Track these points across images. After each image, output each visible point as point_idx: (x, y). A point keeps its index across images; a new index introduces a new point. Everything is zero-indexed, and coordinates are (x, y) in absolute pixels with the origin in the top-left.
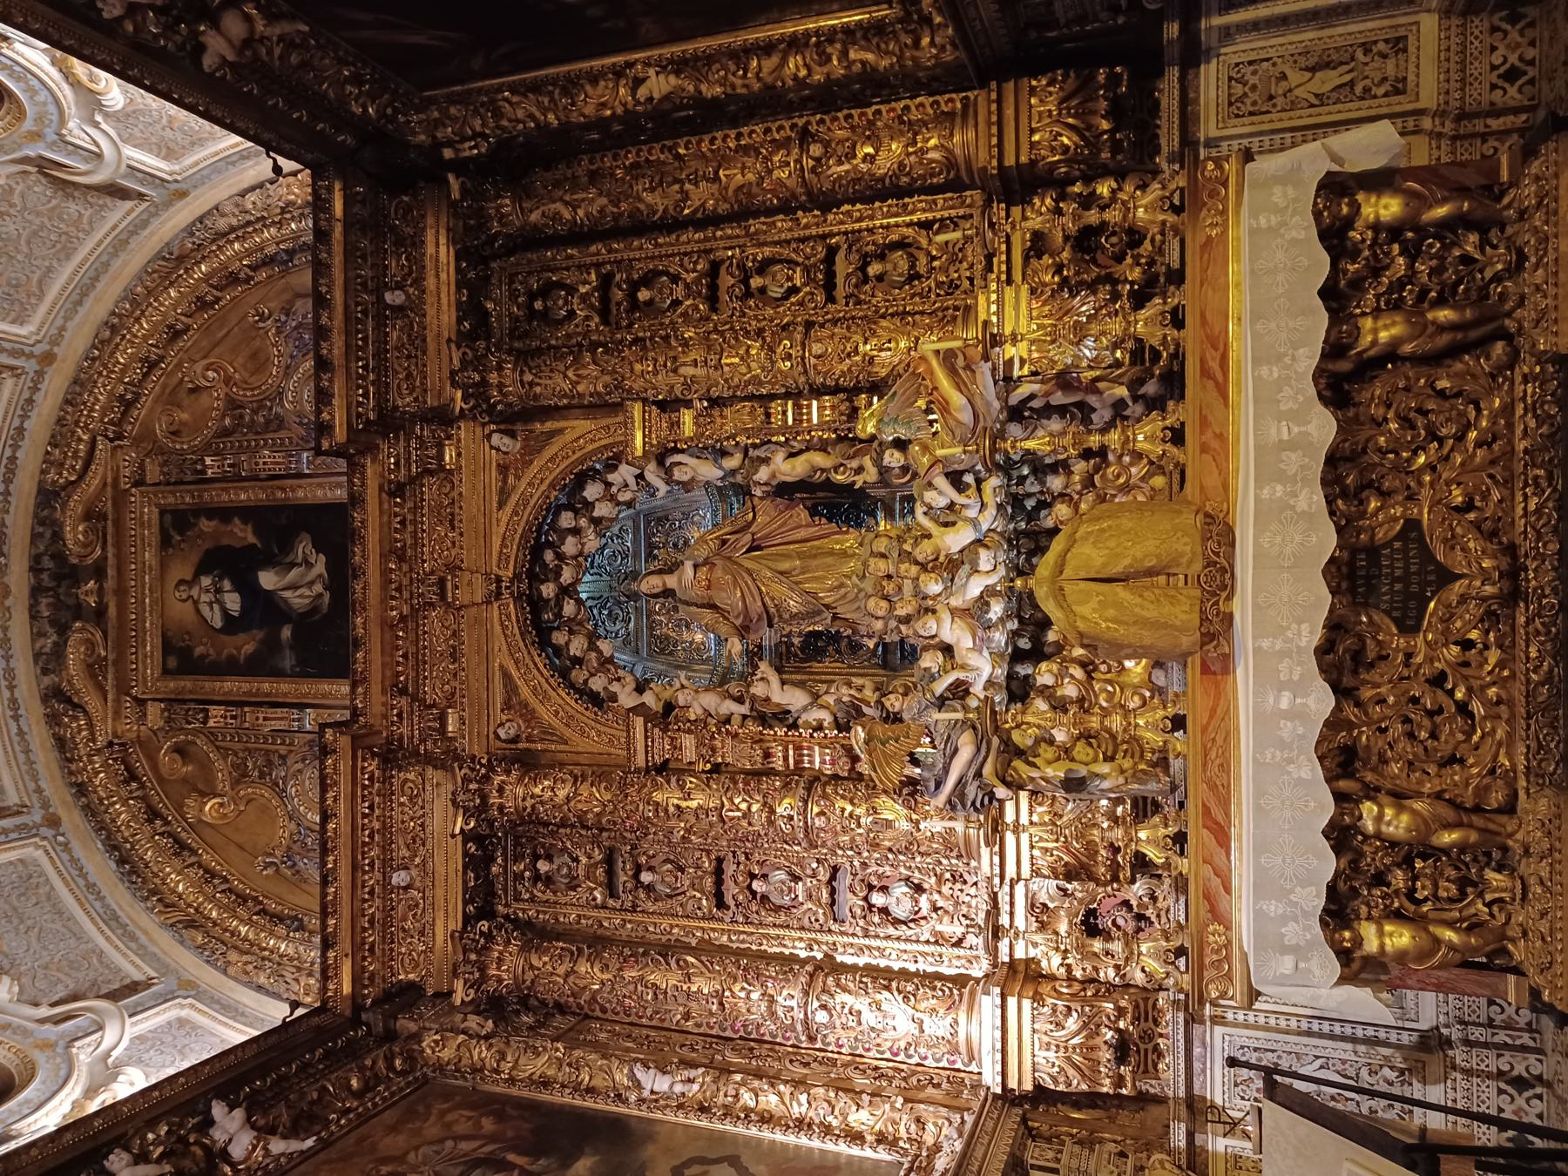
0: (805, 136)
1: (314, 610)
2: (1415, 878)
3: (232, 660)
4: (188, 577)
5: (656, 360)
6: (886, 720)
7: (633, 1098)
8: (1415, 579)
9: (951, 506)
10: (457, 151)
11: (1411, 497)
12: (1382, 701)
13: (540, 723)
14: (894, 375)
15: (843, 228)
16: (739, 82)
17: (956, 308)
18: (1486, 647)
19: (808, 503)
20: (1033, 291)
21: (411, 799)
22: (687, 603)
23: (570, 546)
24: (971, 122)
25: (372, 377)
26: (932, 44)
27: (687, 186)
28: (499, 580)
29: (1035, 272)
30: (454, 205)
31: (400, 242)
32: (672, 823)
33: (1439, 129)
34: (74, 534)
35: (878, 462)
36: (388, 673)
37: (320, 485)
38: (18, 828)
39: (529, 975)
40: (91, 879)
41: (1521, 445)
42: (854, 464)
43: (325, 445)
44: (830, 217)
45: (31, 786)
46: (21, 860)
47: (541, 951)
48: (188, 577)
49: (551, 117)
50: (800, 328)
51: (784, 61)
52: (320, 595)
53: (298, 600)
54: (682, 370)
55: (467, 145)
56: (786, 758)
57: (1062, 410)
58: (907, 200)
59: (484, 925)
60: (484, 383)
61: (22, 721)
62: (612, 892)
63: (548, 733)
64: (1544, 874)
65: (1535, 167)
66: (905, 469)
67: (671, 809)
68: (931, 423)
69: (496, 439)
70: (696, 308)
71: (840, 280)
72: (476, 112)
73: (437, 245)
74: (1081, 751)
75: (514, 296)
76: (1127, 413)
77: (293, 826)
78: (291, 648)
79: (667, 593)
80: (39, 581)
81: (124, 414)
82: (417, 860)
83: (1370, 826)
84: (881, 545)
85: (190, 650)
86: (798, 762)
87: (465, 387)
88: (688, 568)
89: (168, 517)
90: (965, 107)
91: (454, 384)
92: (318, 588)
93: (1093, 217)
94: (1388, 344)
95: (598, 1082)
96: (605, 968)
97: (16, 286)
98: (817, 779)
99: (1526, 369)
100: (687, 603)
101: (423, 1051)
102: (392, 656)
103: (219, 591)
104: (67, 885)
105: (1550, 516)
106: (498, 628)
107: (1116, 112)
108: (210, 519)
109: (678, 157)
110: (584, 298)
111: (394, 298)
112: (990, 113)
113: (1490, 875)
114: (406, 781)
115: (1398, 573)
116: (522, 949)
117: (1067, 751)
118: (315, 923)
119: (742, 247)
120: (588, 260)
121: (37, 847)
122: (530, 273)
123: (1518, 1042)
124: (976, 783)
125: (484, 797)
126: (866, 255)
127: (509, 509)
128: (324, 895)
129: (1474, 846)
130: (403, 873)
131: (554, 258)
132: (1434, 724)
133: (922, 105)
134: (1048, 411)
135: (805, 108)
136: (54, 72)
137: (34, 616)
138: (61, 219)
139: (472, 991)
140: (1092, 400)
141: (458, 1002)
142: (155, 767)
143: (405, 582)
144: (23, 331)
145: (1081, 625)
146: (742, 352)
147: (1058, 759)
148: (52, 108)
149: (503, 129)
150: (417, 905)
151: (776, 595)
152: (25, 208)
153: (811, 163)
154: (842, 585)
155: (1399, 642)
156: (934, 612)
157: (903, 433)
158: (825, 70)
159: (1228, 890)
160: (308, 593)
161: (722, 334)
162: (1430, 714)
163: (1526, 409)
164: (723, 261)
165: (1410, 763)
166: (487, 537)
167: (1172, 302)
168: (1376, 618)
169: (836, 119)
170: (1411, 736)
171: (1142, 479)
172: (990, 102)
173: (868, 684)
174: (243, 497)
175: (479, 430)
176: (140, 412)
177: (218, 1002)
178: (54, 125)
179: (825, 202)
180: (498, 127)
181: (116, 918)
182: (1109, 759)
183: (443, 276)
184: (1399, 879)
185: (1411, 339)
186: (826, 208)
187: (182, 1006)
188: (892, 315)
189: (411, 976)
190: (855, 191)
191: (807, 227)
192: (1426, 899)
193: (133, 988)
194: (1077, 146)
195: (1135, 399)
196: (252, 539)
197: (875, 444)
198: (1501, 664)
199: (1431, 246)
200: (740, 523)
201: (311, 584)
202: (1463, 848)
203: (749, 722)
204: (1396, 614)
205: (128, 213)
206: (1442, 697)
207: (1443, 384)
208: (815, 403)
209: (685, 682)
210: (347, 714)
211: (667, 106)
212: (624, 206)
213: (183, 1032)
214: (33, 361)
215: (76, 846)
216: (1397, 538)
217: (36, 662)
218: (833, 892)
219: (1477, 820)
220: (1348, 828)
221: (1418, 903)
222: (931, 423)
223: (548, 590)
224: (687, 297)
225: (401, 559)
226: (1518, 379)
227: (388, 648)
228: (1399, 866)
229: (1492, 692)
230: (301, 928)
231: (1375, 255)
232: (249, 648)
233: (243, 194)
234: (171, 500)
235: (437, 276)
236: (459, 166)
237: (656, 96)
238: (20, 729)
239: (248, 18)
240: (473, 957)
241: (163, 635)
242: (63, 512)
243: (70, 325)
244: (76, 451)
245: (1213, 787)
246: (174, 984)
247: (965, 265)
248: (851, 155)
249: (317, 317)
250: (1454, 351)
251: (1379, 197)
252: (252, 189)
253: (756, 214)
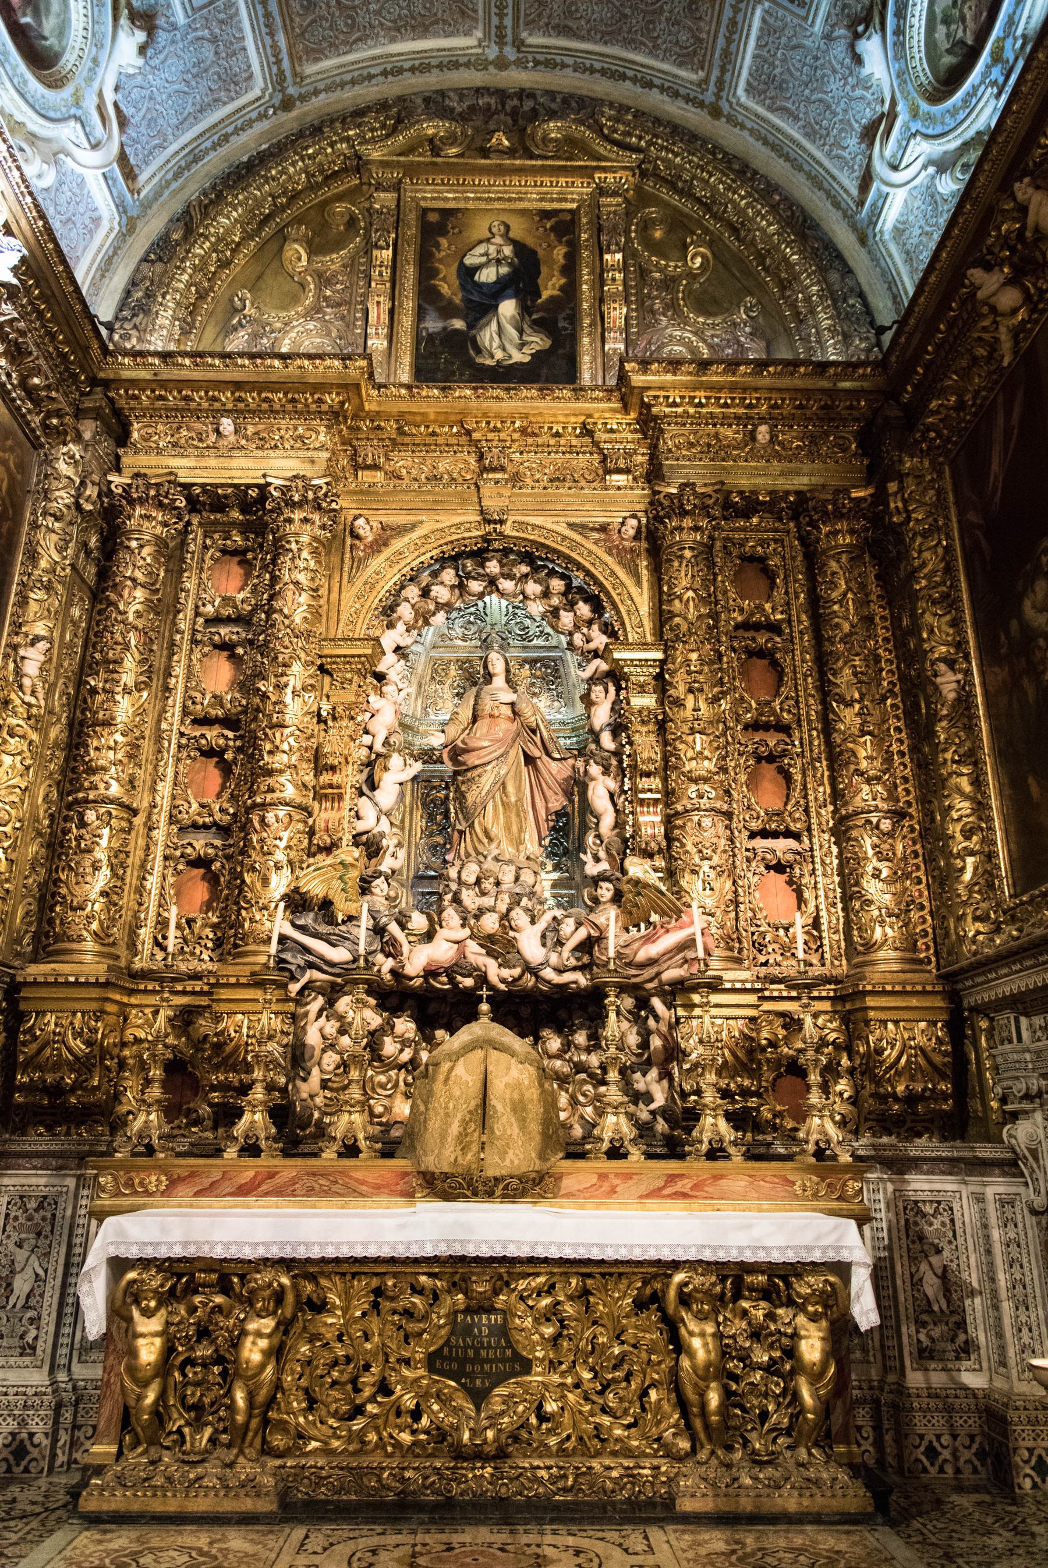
0: (899, 815)
1: (478, 351)
2: (204, 1365)
3: (433, 273)
4: (511, 235)
5: (700, 673)
6: (363, 880)
7: (17, 639)
8: (477, 1368)
10: (896, 494)
11: (553, 1365)
12: (367, 1337)
13: (367, 557)
14: (679, 892)
15: (816, 847)
16: (948, 755)
17: (740, 950)
18: (414, 1432)
19: (569, 809)
20: (753, 1019)
21: (301, 437)
22: (477, 696)
23: (533, 588)
24: (907, 967)
25: (692, 411)
26: (978, 933)
27: (857, 706)
28: (501, 522)
29: (770, 1023)
30: (846, 491)
31: (813, 441)
32: (273, 680)
33: (887, 1388)
34: (554, 129)
35: (602, 877)
36: (418, 419)
37: (594, 359)
38: (281, 73)
39: (134, 544)
40: (233, 139)
41: (595, 1464)
42: (602, 854)
43: (628, 366)
44: (826, 836)
45: (321, 86)
46: (251, 76)
47: (157, 555)
48: (511, 235)
49: (924, 583)
50: (725, 807)
51: (966, 797)
52: (492, 357)
53: (488, 336)
54: (691, 697)
55: (900, 504)
56: (331, 786)
57: (644, 1045)
58: (840, 906)
59: (181, 503)
60: (684, 514)
61: (381, 79)
62: (210, 621)
63: (359, 564)
64: (206, 1482)
65: (843, 1476)
66: (596, 901)
67: (284, 679)
68: (637, 926)
69: (634, 522)
70: (748, 711)
71: (769, 843)
72: (929, 514)
73: (811, 474)
74: (331, 1060)
75: (763, 543)
76: (641, 1105)
77: (278, 325)
78: (445, 329)
79: (489, 677)
80: (510, 97)
81: (666, 181)
82: (243, 442)
83: (252, 1326)
84: (527, 877)
85: (444, 233)
86: (326, 796)
87: (680, 496)
88: (511, 697)
89: (568, 217)
90: (920, 962)
91: (682, 487)
92: (499, 355)
93: (814, 1078)
94: (689, 1346)
95: (33, 606)
96: (139, 615)
97: (781, 87)
98: (310, 815)
99: (663, 1469)
100: (477, 696)
101: (65, 444)
102: (434, 421)
103: (498, 262)
104: (229, 116)
105: (530, 1489)
106: (457, 520)
107: (911, 1099)
108: (566, 256)
109: (884, 699)
110: (760, 608)
111: (763, 432)
112: (914, 984)
113: (208, 1432)
114: (318, 433)
115: (483, 1353)
116: (157, 537)
117: (332, 1046)
118: (189, 346)
119: (802, 755)
120: (794, 613)
121: (264, 91)
122: (784, 558)
123: (59, 1452)
124: (302, 963)
125: (300, 505)
126: (791, 867)
127: (568, 532)
128: (212, 355)
129: (233, 1420)
130: (231, 428)
131: (796, 581)
132: (344, 1384)
133: (925, 921)
134: (645, 1035)
135: (925, 815)
136: (971, 133)
137: (478, 91)
138: (841, 130)
139: (120, 491)
140: (654, 1073)
141: (110, 478)
142: (339, 198)
143: (503, 436)
144: (740, 91)
145: (445, 1066)
146: (706, 753)
147: (324, 1037)
148: (939, 130)
149: (913, 539)
150: (201, 440)
151: (484, 779)
152: (851, 99)
153: (875, 820)
154: (490, 839)
155: (420, 1353)
156: (463, 926)
158: (958, 835)
159: (197, 1194)
160: (495, 344)
161: (724, 734)
162: (354, 1381)
163: (628, 1468)
164: (790, 736)
165: (309, 1363)
166: (541, 512)
167: (732, 1150)
168: (443, 1332)
169: (914, 843)
170: (335, 1363)
171: (582, 1117)
172: (924, 985)
173: (397, 864)
174: (585, 287)
175: (642, 507)
176: (664, 194)
177: (115, 253)
178: (924, 130)
179: (841, 831)
180: (915, 534)
181: (195, 161)
182: (324, 1084)
183: (781, 480)
184: (204, 1351)
185: (694, 1367)
186: (833, 832)
187: (111, 220)
188: (736, 892)
189: (135, 435)
190: (848, 860)
191: (818, 814)
192: (185, 1375)
193: (130, 174)
194: (882, 1063)
195: (653, 1113)
196: (545, 295)
197: (618, 874)
198: (398, 1445)
199: (777, 1384)
200: (551, 747)
201: (504, 349)
202: (232, 1408)
203: (364, 752)
204: (446, 1350)
205: (846, 191)
206: (367, 1392)
207: (653, 1395)
208: (658, 819)
209: (403, 694)
210: (379, 378)
211: (930, 690)
212: (841, 647)
213: (87, 222)
214: (713, 99)
215: (264, 125)
216: (515, 1353)
217: (437, 92)
218: (205, 827)
219: (254, 1423)
220: (251, 1305)
221: (182, 1368)
222: (637, 926)
223: (493, 567)
224: (758, 703)
225: (523, 431)
226: (655, 1462)
227: (442, 418)
228: (216, 1351)
229: (372, 1437)
230: (185, 333)
231: (771, 1334)
232: (445, 289)
233: (862, 295)
234: (584, 220)
235: (782, 474)
236: (881, 497)
237: (939, 680)
238: (374, 76)
239: (1014, 311)
240: (152, 493)
241: (458, 210)
242: (574, 121)
243: (746, 133)
244: (629, 134)
245: (293, 1181)
246: (134, 212)
247: (779, 958)
248: (880, 856)
249: (748, 362)
250: (682, 1404)
251: (823, 1339)
252: (866, 304)
253: (831, 768)
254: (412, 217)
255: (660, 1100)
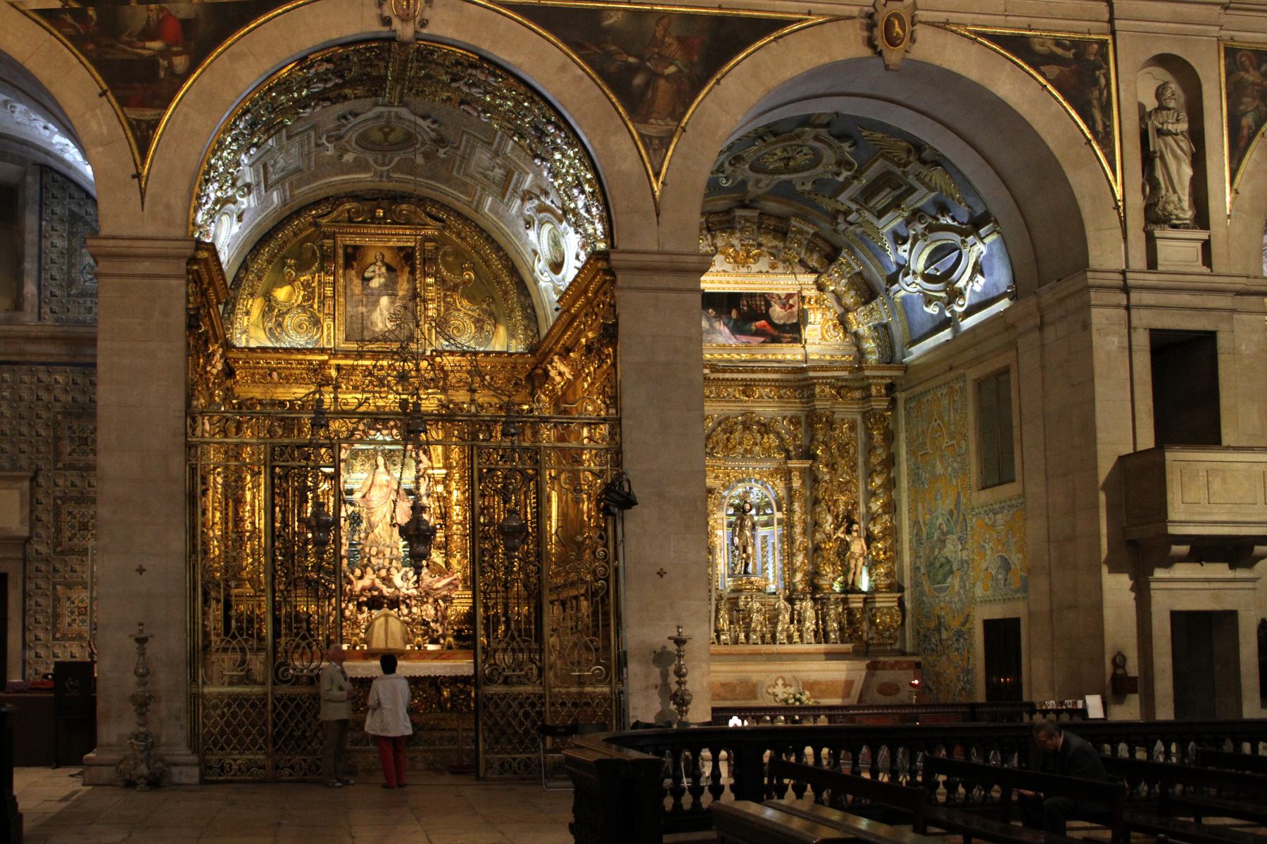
4: (385, 260)
9: (408, 579)
48: (385, 260)
57: (436, 614)
85: (355, 259)
134: (436, 609)
144: (486, 210)
157: (431, 566)
254: (341, 252)
255: (440, 632)
